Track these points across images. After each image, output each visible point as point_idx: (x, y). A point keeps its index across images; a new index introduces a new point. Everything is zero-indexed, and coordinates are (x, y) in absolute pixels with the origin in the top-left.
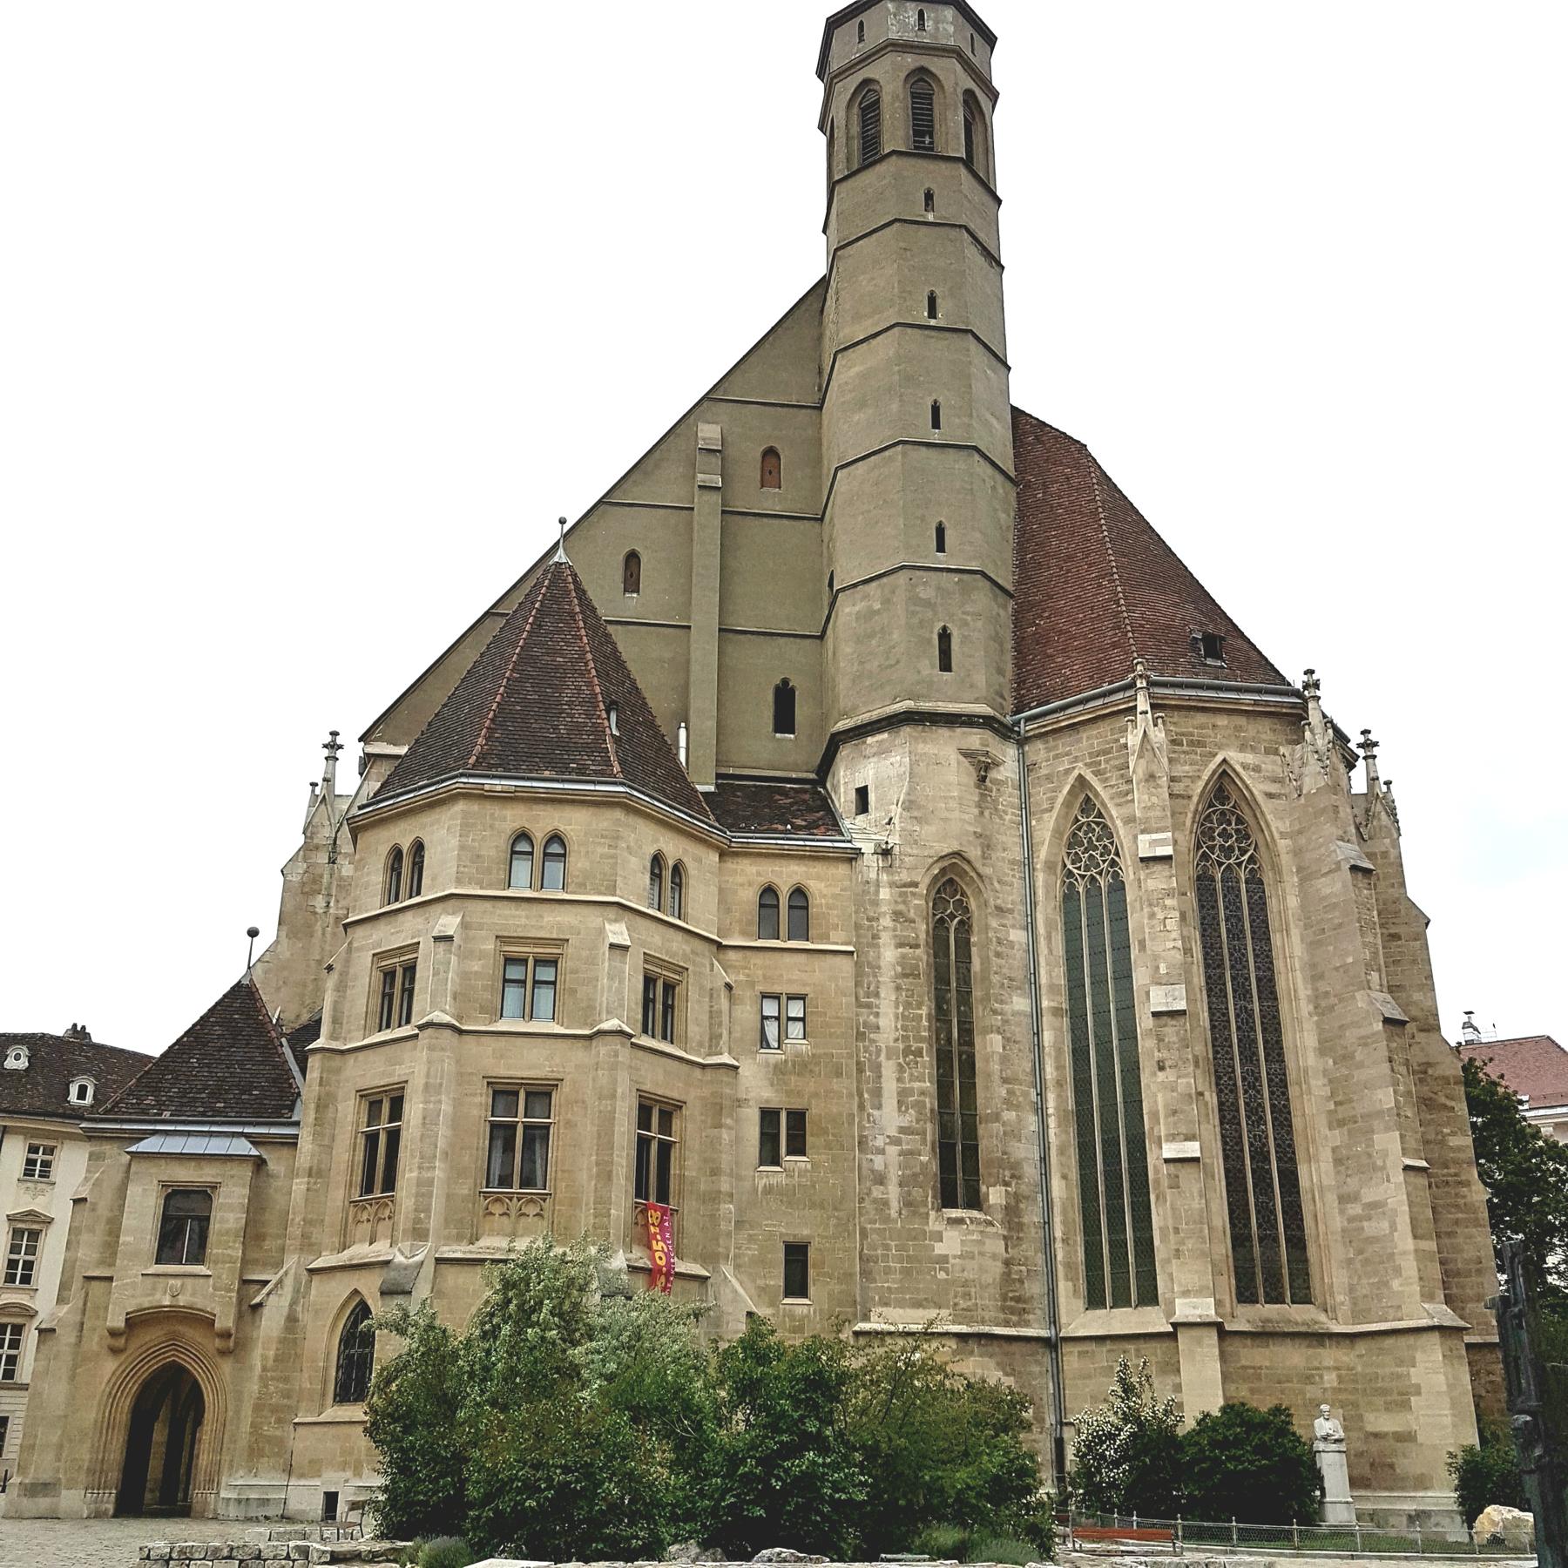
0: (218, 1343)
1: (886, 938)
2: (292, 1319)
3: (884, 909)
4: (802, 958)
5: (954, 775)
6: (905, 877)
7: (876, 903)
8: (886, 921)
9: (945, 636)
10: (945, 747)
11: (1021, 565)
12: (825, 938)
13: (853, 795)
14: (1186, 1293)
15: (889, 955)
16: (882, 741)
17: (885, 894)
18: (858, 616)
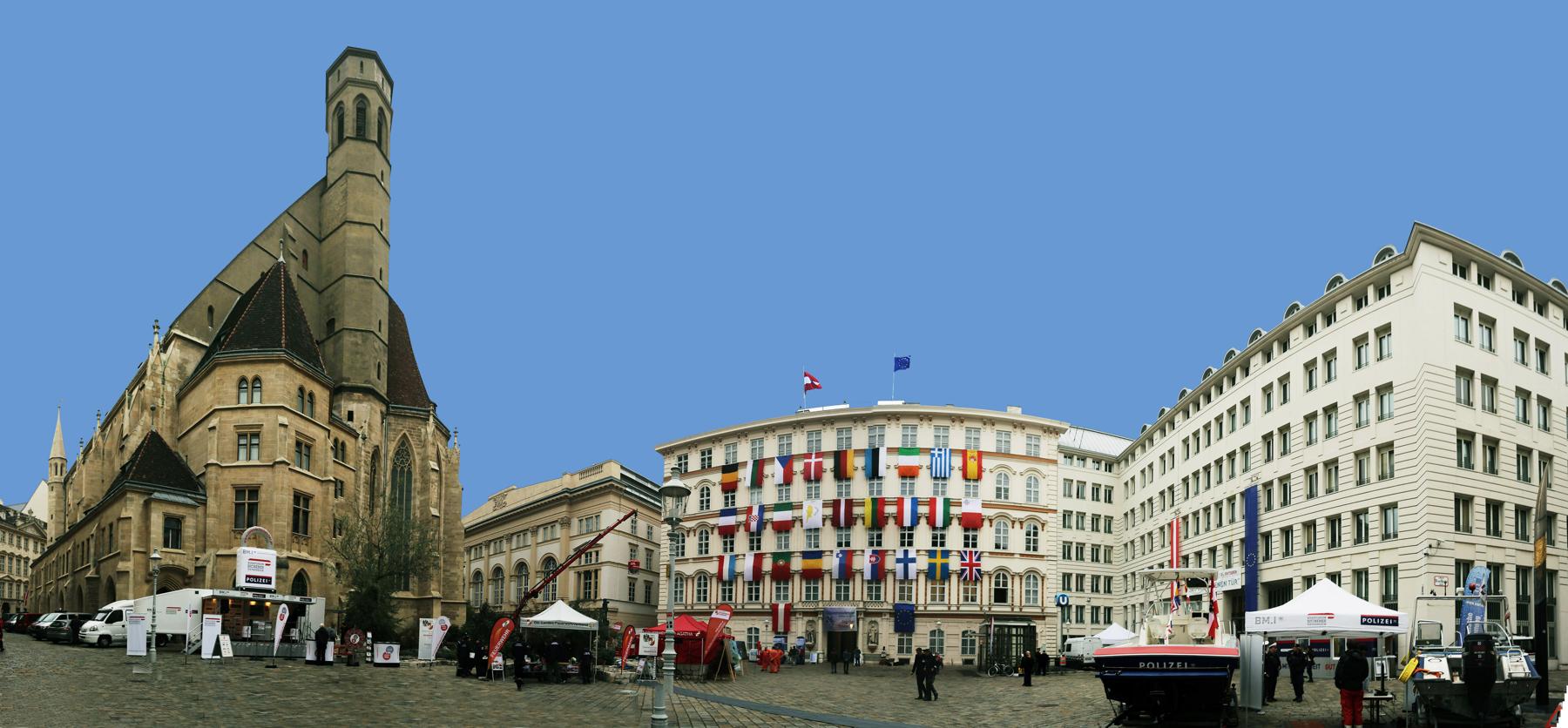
0: (187, 581)
1: (362, 468)
2: (213, 573)
3: (363, 458)
4: (343, 468)
5: (378, 418)
6: (368, 449)
7: (361, 456)
8: (363, 463)
9: (379, 366)
10: (379, 407)
11: (389, 340)
12: (349, 464)
13: (347, 413)
14: (434, 590)
15: (363, 475)
16: (359, 396)
17: (363, 453)
18: (352, 343)
